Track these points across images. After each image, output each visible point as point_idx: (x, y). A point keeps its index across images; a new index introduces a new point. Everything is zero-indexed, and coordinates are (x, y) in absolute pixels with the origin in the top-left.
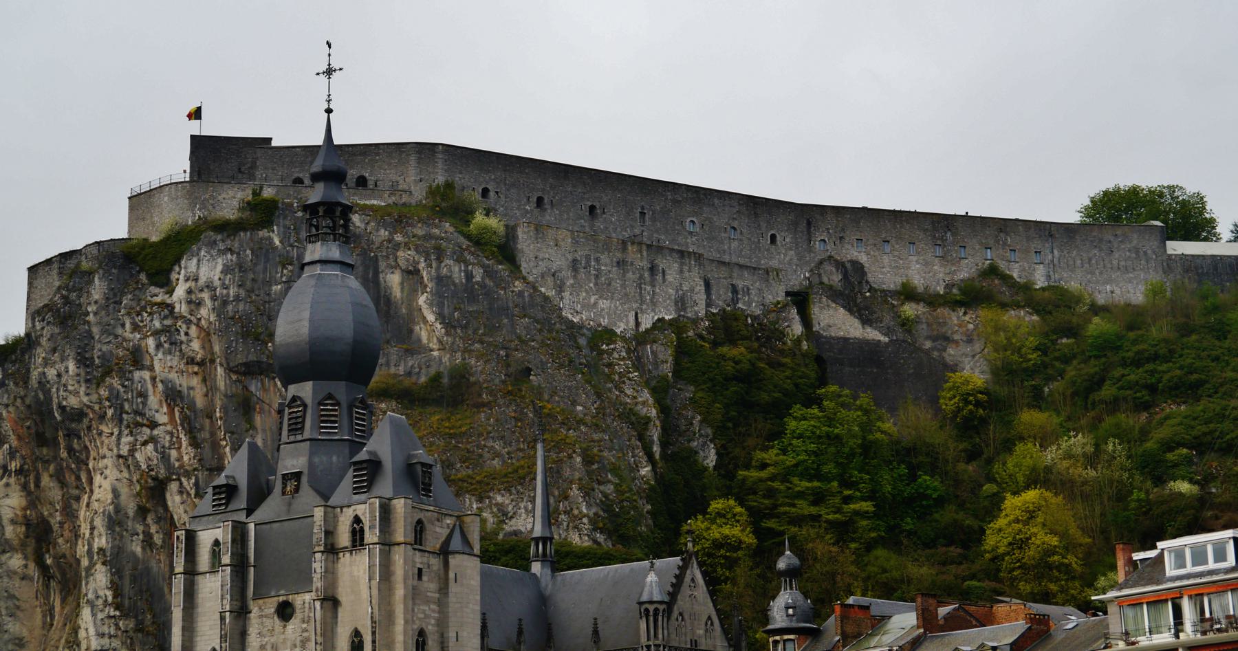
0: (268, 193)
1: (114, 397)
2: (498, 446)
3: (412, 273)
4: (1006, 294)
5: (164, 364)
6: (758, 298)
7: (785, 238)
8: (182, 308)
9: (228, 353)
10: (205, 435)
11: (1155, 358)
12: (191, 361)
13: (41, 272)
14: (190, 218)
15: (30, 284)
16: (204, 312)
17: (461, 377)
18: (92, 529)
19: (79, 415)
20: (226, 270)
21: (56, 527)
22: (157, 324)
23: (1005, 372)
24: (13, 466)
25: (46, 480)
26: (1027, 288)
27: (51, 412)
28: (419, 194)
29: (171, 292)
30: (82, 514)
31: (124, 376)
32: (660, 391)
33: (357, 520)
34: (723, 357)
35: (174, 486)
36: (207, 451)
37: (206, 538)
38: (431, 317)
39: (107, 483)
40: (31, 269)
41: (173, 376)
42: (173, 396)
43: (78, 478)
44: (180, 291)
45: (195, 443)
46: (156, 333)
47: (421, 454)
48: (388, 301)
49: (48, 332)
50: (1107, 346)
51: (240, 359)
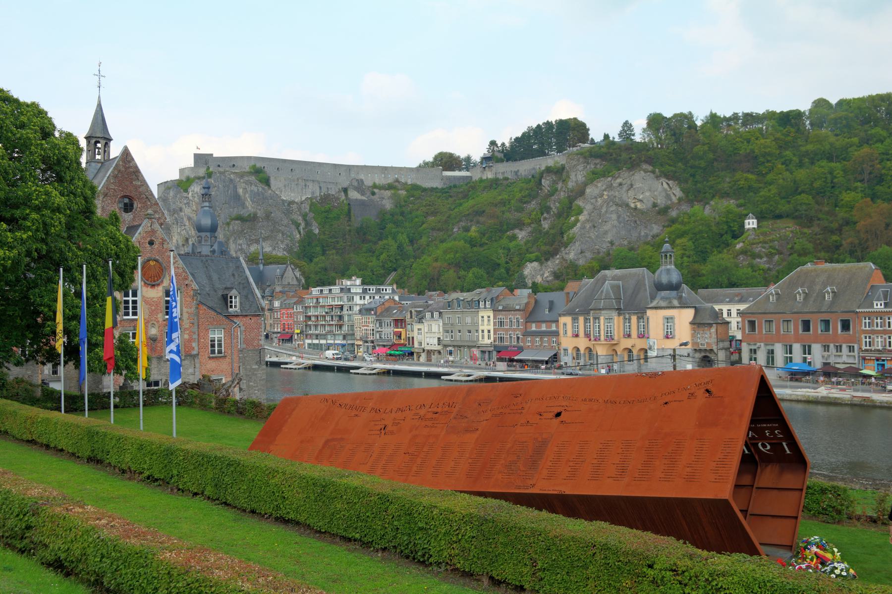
0: (211, 170)
1: (176, 219)
3: (245, 189)
4: (399, 187)
5: (187, 211)
8: (191, 198)
17: (255, 215)
32: (304, 216)
42: (189, 219)
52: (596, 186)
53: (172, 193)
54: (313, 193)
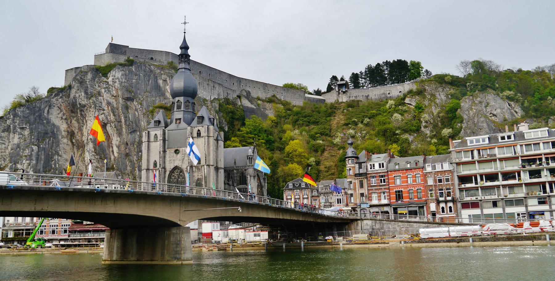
0: (131, 58)
3: (165, 81)
5: (106, 96)
6: (232, 96)
7: (236, 84)
8: (111, 83)
9: (123, 94)
10: (116, 113)
11: (309, 116)
12: (113, 96)
13: (69, 71)
14: (112, 62)
15: (66, 74)
16: (116, 84)
19: (85, 106)
20: (122, 75)
21: (76, 133)
22: (105, 86)
23: (278, 116)
24: (64, 117)
25: (73, 121)
26: (280, 100)
27: (76, 105)
28: (165, 63)
29: (108, 79)
30: (84, 130)
31: (96, 97)
33: (199, 130)
34: (228, 108)
35: (109, 125)
36: (117, 117)
37: (152, 134)
40: (67, 71)
41: (108, 99)
42: (109, 104)
44: (110, 79)
45: (114, 115)
46: (104, 88)
47: (212, 117)
48: (160, 87)
49: (76, 85)
50: (297, 113)
51: (126, 96)
52: (466, 102)
53: (89, 76)
54: (219, 95)
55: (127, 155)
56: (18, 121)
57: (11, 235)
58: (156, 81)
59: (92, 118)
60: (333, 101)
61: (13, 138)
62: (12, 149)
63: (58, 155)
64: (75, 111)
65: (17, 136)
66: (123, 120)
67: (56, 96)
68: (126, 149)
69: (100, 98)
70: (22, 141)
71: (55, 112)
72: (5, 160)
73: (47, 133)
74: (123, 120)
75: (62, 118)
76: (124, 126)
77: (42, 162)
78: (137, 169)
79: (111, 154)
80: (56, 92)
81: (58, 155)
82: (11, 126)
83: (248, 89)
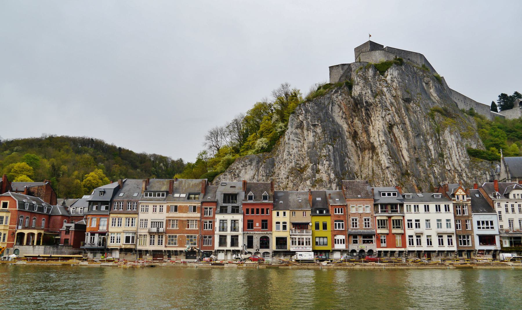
0: (398, 57)
2: (461, 127)
5: (388, 95)
8: (389, 82)
15: (330, 71)
16: (394, 84)
18: (379, 135)
20: (398, 74)
21: (359, 134)
22: (385, 85)
24: (344, 116)
25: (356, 121)
28: (421, 66)
29: (386, 77)
38: (435, 95)
39: (378, 124)
40: (330, 67)
43: (368, 121)
44: (389, 78)
51: (406, 97)
53: (371, 72)
55: (418, 160)
56: (310, 117)
57: (507, 245)
58: (422, 85)
59: (380, 118)
60: (518, 118)
61: (308, 135)
62: (309, 148)
63: (348, 157)
64: (359, 108)
65: (311, 134)
66: (408, 123)
67: (336, 92)
68: (415, 153)
69: (384, 97)
70: (316, 139)
71: (336, 109)
72: (303, 160)
73: (335, 132)
74: (408, 123)
75: (342, 117)
76: (409, 128)
77: (339, 164)
78: (432, 176)
79: (402, 158)
80: (336, 89)
81: (348, 157)
82: (304, 122)
83: (455, 101)
